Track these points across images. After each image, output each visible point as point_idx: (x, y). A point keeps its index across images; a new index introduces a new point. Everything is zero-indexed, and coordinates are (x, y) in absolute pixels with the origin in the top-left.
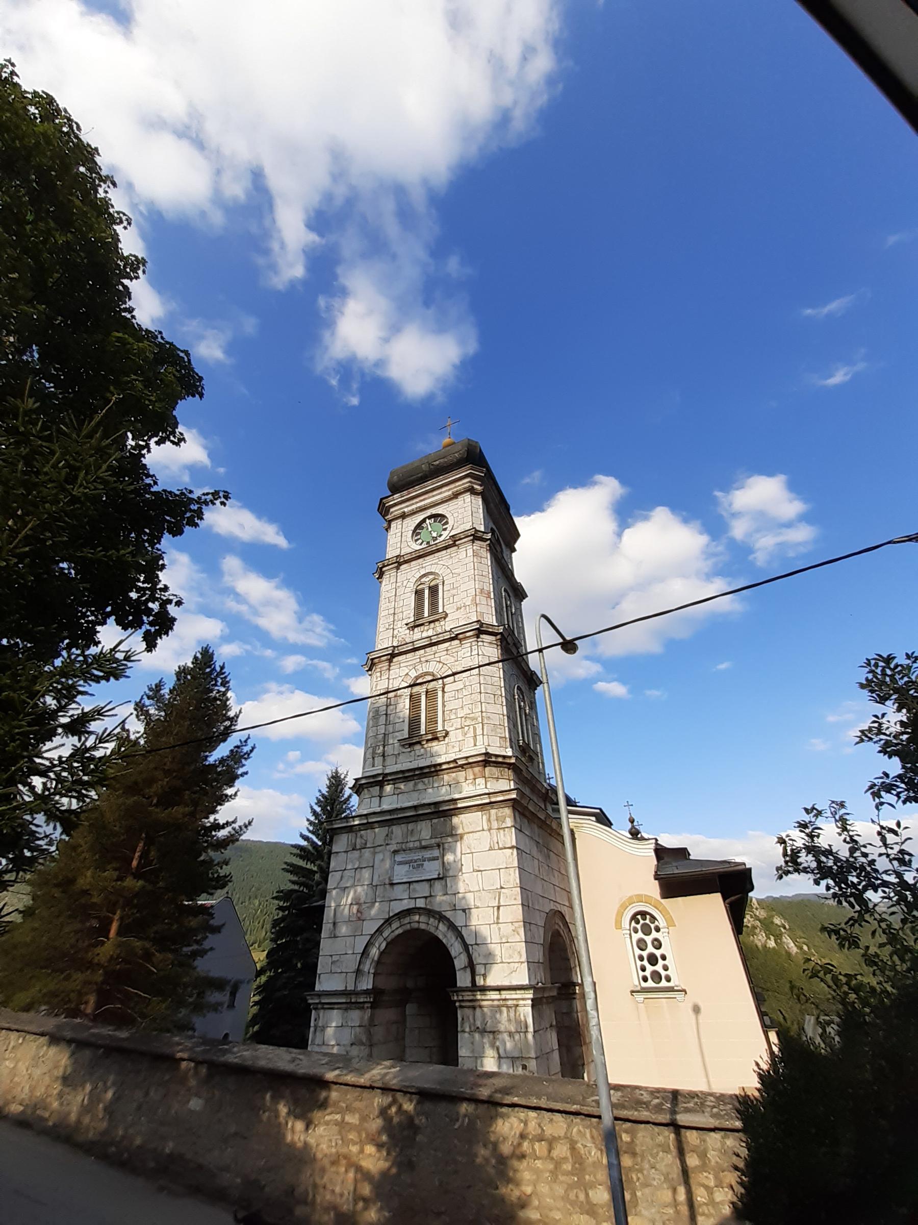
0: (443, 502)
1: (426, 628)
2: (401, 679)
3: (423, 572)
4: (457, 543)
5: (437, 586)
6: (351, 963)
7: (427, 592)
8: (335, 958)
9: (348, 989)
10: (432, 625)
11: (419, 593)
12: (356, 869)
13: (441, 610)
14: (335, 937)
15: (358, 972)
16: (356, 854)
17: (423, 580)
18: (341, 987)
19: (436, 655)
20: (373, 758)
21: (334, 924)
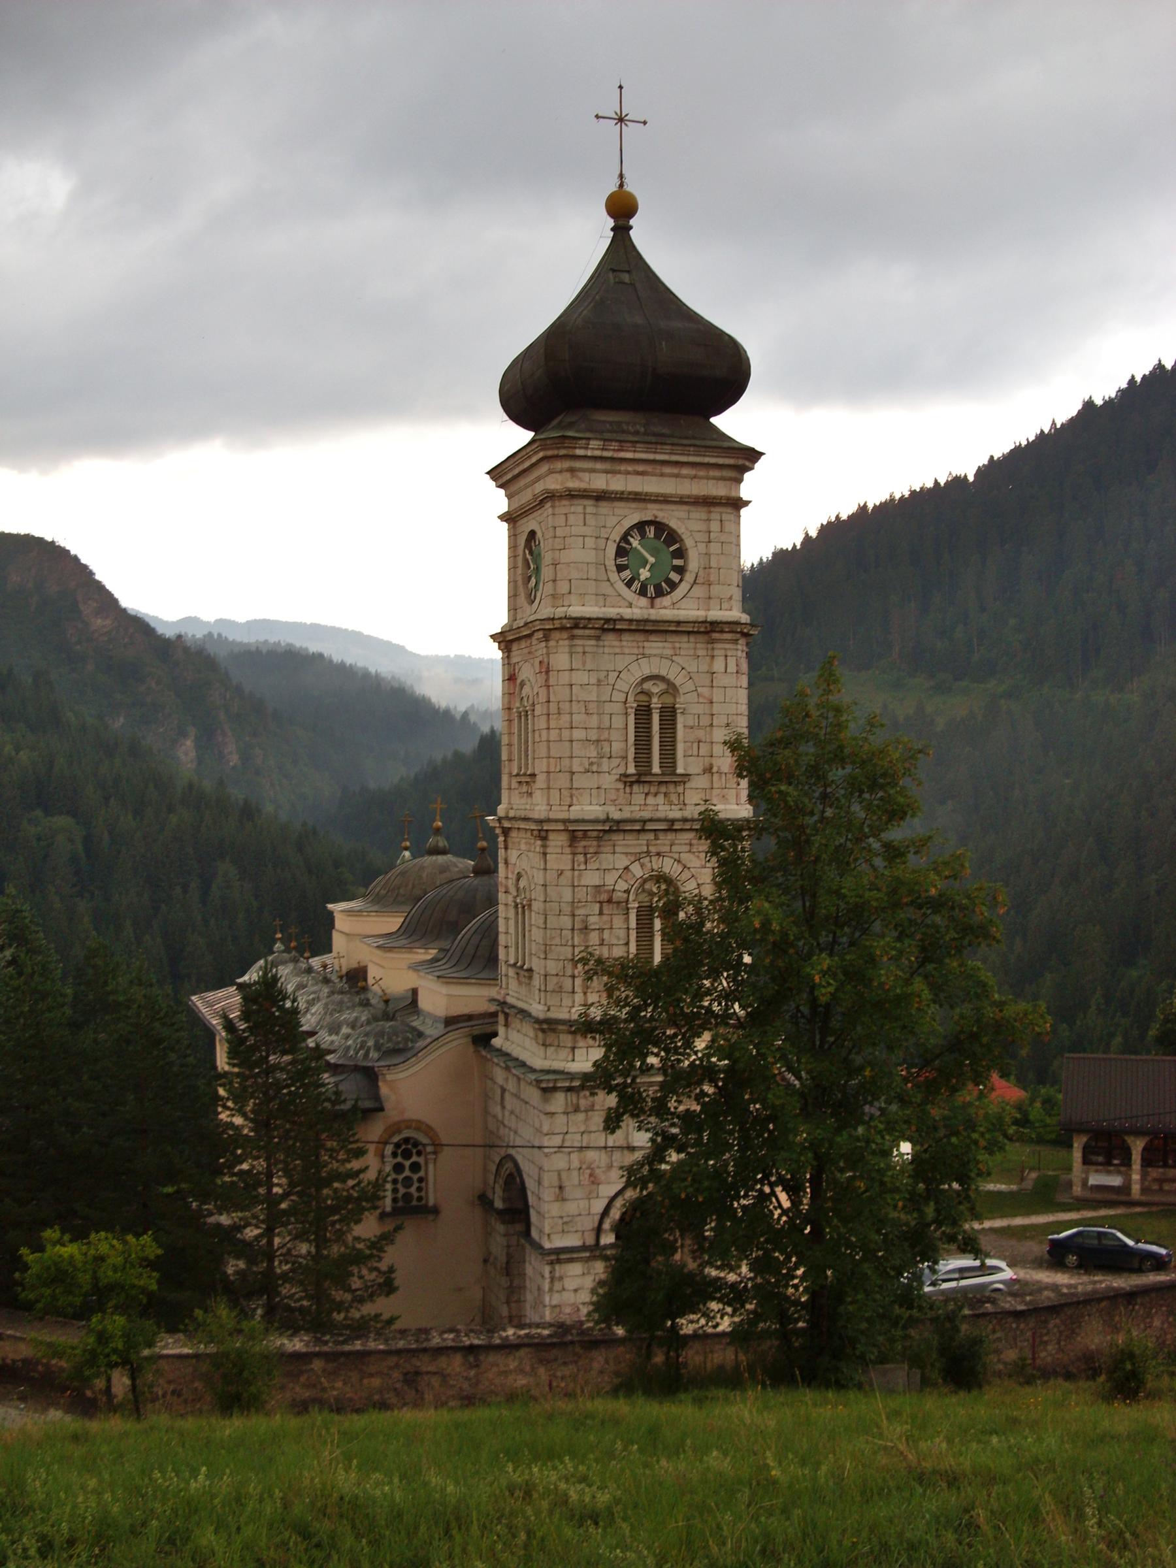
0: (683, 501)
1: (653, 789)
2: (616, 874)
3: (647, 672)
4: (715, 635)
5: (673, 710)
6: (590, 1223)
7: (656, 718)
8: (565, 1219)
9: (588, 1244)
10: (663, 789)
11: (643, 713)
12: (583, 1133)
13: (680, 770)
14: (564, 1200)
15: (599, 1230)
16: (581, 1116)
17: (646, 686)
18: (578, 1243)
19: (675, 848)
20: (585, 993)
21: (561, 1188)
